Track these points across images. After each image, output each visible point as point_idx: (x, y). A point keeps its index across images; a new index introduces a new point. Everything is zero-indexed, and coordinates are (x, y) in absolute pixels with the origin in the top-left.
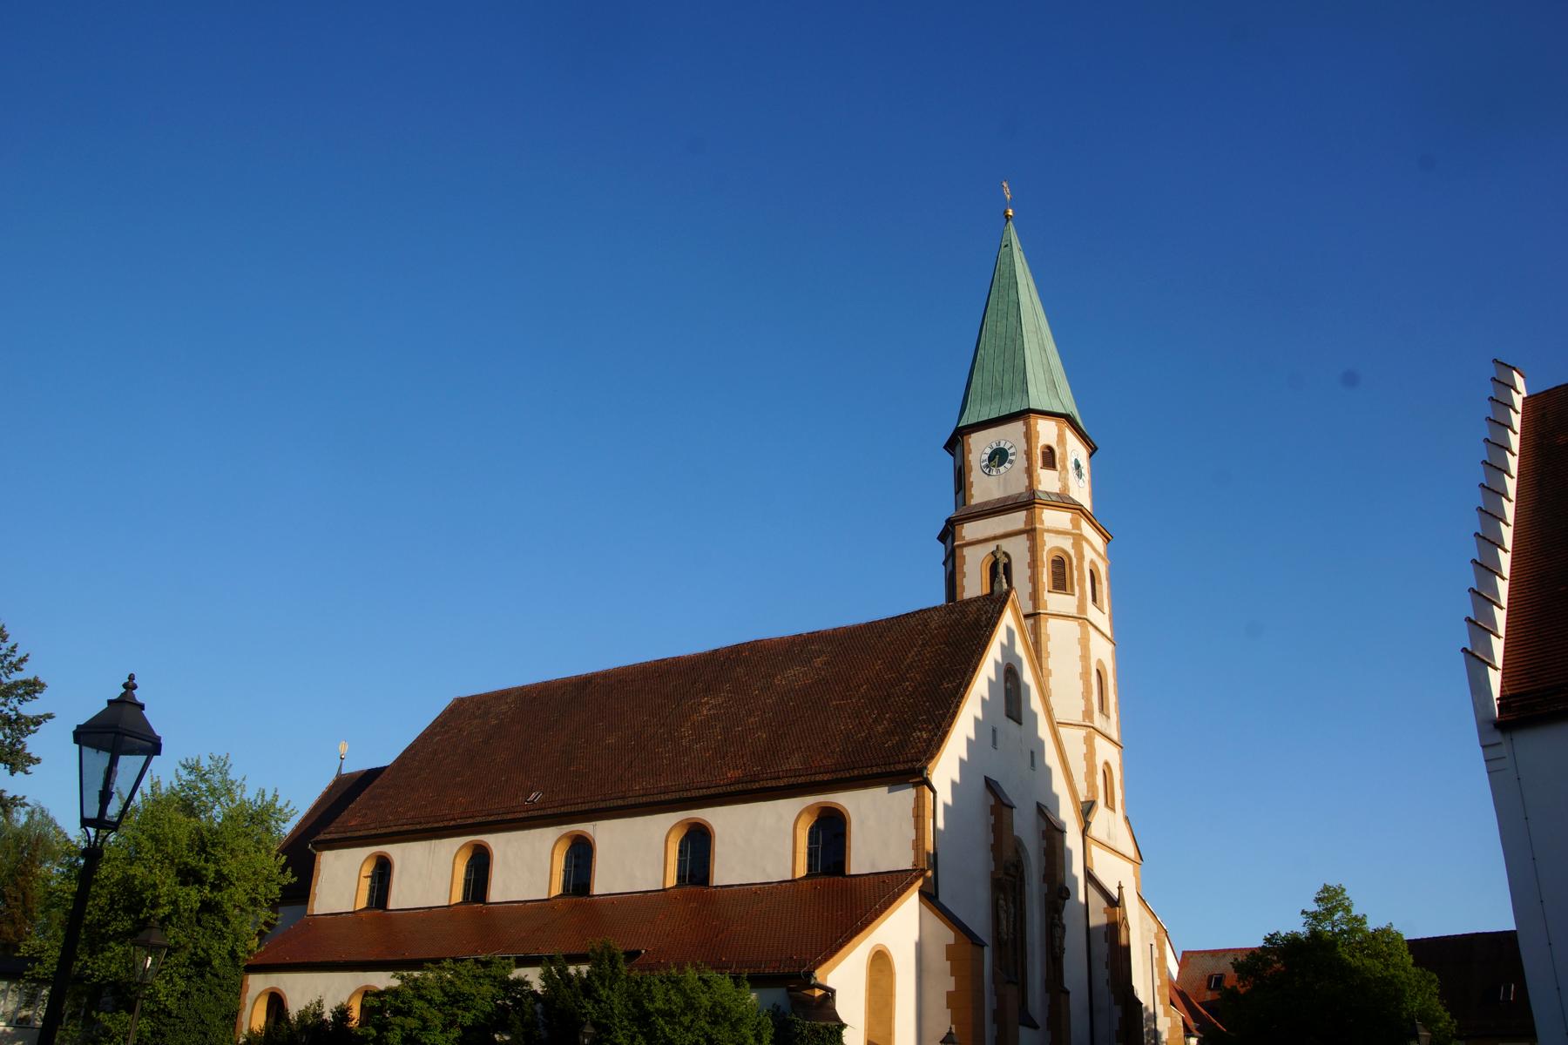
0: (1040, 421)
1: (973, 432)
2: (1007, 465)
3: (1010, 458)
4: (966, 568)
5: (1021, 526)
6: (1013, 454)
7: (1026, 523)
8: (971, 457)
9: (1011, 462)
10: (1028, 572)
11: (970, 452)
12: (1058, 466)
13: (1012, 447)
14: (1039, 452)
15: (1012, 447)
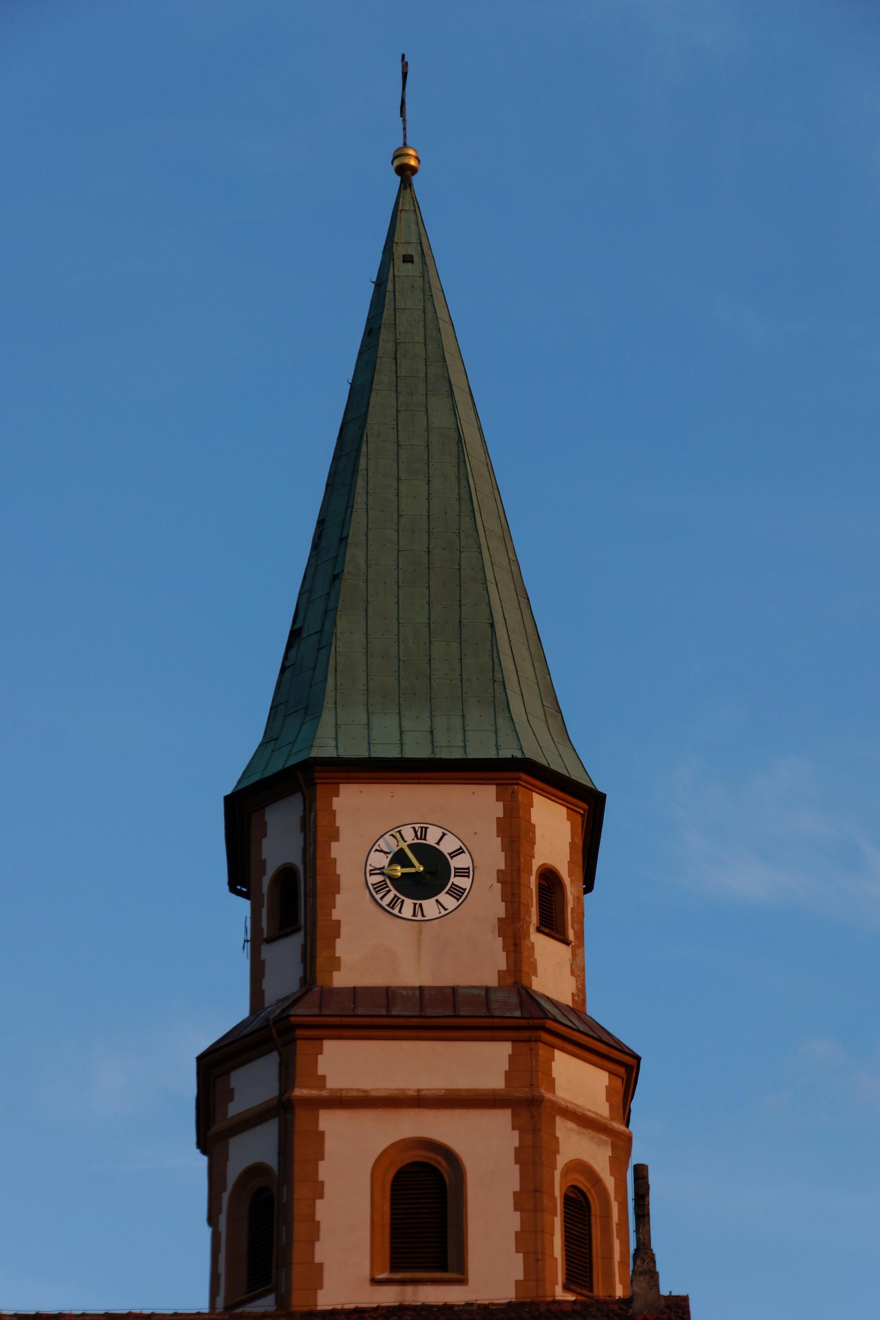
0: (537, 799)
1: (349, 780)
2: (444, 897)
3: (453, 880)
4: (324, 1171)
5: (495, 1081)
6: (463, 872)
7: (509, 1076)
8: (336, 850)
9: (457, 893)
10: (513, 1221)
11: (334, 835)
12: (571, 935)
13: (459, 852)
14: (533, 880)
15: (459, 852)
